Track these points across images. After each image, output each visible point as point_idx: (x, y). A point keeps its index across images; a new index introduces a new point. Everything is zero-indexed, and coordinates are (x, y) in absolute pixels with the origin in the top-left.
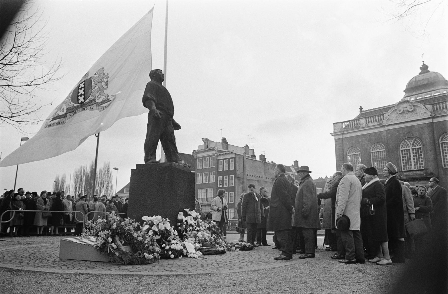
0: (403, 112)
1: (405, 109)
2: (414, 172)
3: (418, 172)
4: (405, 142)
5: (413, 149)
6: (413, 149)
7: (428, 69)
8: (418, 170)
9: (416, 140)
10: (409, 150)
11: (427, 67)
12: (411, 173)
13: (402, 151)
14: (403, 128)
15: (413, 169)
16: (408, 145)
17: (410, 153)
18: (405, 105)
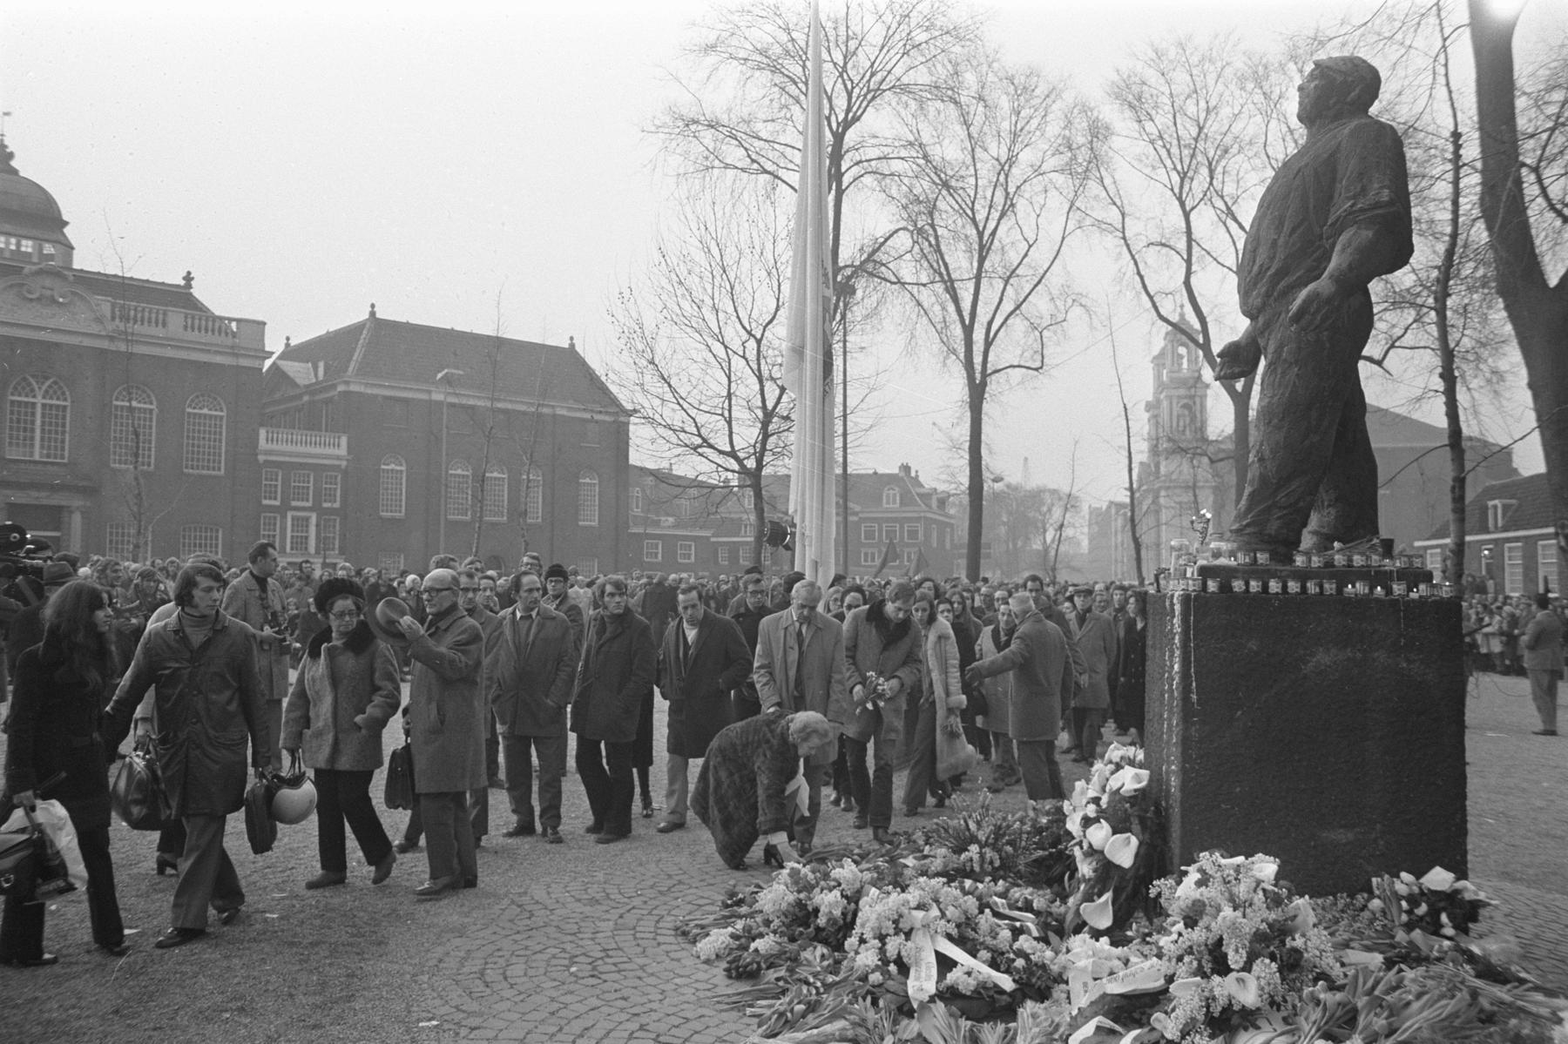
0: (39, 299)
1: (48, 293)
2: (39, 467)
3: (50, 468)
4: (25, 379)
5: (44, 405)
6: (44, 405)
7: (14, 163)
8: (52, 464)
9: (55, 383)
10: (34, 404)
11: (11, 155)
12: (32, 466)
13: (12, 402)
14: (28, 342)
15: (37, 457)
16: (32, 390)
17: (33, 414)
18: (48, 282)
